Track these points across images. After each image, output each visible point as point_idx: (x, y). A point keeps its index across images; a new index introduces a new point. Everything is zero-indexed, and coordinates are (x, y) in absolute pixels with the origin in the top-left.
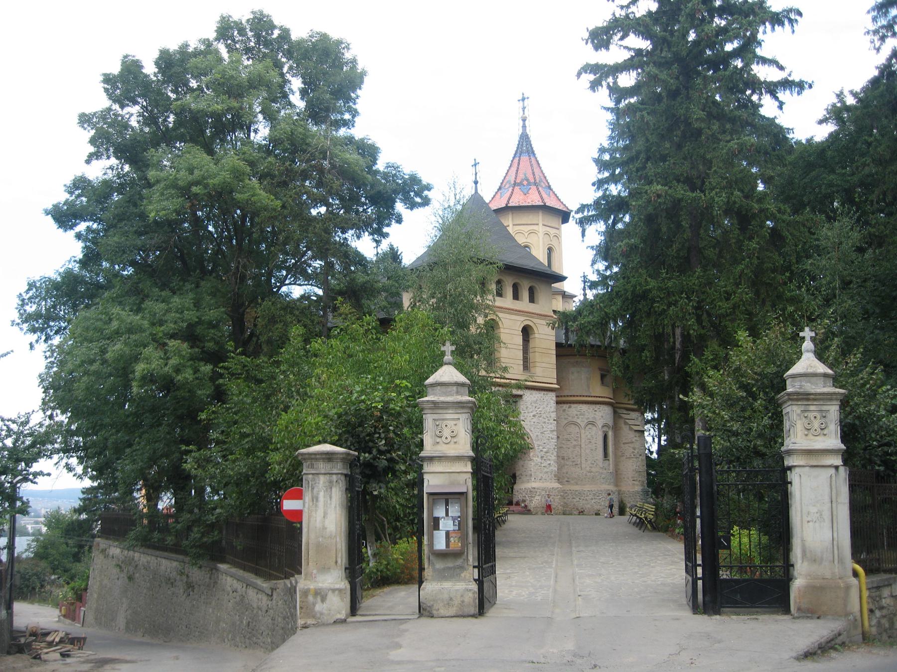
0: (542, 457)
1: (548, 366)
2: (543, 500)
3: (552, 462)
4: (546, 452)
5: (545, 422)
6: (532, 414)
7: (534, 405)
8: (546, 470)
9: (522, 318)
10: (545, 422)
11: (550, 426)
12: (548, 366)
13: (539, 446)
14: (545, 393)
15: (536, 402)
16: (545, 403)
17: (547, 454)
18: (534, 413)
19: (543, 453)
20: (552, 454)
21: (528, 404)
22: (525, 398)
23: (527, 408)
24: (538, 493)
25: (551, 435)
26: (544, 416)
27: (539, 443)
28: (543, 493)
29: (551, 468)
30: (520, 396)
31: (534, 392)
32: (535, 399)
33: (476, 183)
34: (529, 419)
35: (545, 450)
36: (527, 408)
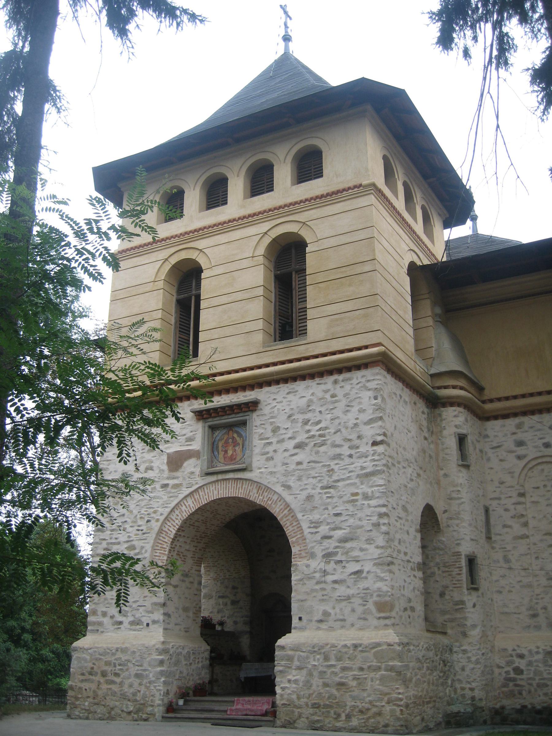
0: (328, 556)
1: (349, 306)
2: (316, 682)
3: (368, 567)
4: (344, 540)
5: (338, 457)
6: (293, 443)
7: (301, 417)
8: (342, 590)
9: (265, 227)
10: (338, 457)
11: (359, 463)
12: (349, 306)
13: (316, 524)
14: (341, 377)
15: (308, 408)
16: (341, 405)
17: (348, 545)
18: (302, 437)
19: (331, 545)
20: (369, 541)
21: (281, 421)
22: (265, 409)
23: (276, 430)
24: (296, 663)
25: (364, 488)
26: (338, 439)
27: (316, 516)
28: (315, 661)
29: (362, 585)
30: (253, 406)
31: (300, 386)
32: (304, 401)
33: (287, 39)
34: (279, 457)
35: (338, 534)
36: (276, 430)
